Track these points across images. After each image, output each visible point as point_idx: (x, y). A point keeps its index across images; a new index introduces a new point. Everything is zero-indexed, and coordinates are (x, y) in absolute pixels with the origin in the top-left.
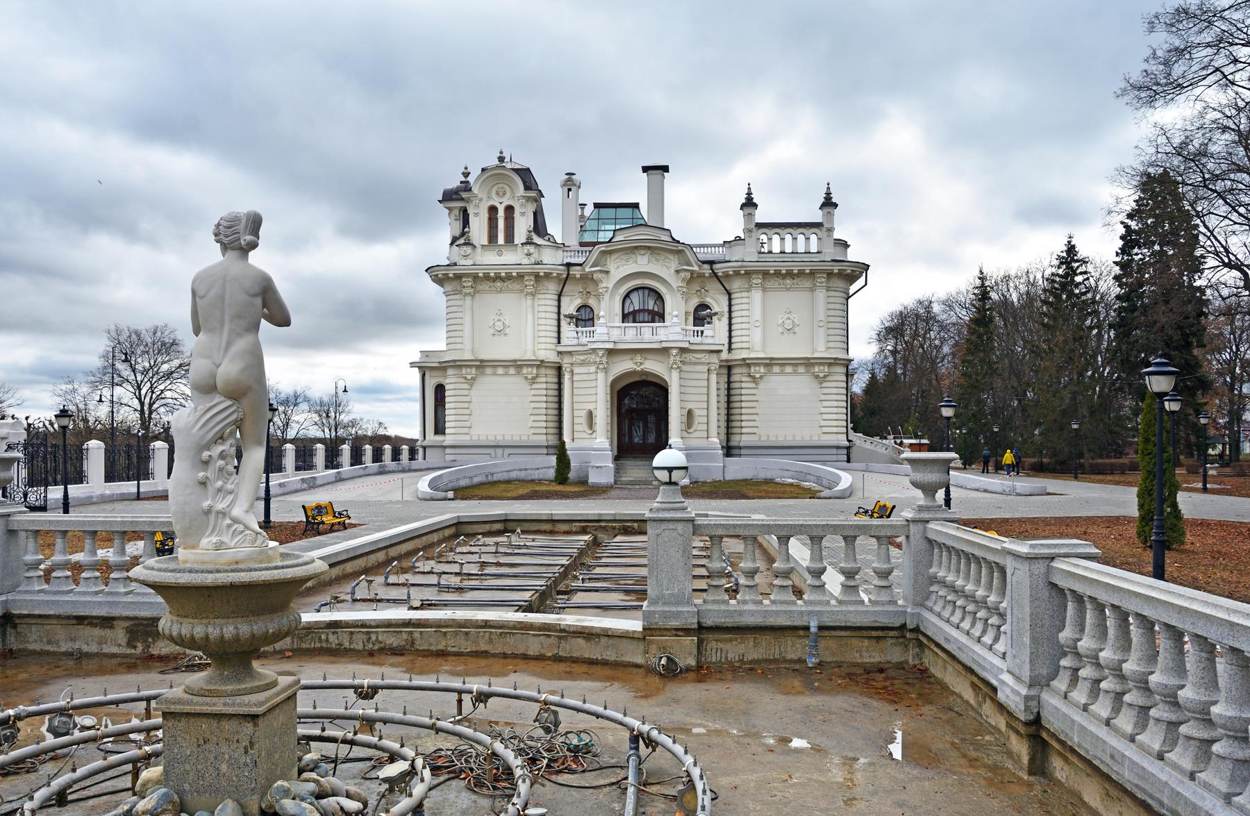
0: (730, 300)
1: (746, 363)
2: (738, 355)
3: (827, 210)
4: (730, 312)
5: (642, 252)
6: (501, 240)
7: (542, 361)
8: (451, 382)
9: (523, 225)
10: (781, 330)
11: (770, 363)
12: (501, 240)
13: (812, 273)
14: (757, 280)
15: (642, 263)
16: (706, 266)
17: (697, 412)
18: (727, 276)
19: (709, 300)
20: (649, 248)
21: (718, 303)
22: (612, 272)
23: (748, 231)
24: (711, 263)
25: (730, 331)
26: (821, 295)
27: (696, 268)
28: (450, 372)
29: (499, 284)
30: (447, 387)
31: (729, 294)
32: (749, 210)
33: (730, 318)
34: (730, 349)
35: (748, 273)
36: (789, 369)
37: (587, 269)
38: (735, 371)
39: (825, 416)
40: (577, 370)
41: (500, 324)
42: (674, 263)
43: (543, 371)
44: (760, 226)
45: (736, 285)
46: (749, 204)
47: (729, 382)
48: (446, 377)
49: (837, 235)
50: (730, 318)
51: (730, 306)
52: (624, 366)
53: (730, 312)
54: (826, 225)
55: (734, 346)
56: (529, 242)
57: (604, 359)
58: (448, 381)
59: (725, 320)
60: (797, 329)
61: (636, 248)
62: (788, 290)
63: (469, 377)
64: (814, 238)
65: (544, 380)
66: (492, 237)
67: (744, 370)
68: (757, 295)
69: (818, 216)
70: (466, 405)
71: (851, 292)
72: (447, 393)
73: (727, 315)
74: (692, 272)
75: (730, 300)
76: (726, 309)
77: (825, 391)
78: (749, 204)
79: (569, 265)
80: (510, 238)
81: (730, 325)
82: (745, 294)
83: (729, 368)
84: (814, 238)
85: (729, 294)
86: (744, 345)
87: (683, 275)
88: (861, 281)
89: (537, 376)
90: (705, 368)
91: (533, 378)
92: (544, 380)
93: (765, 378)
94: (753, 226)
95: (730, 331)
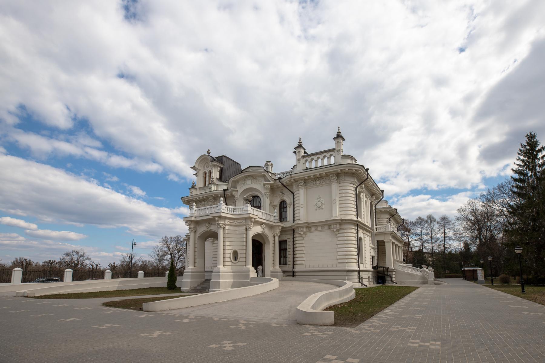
0: (294, 196)
4: (294, 202)
5: (249, 178)
10: (315, 208)
11: (309, 226)
13: (328, 175)
19: (285, 198)
21: (288, 200)
24: (280, 178)
26: (335, 186)
27: (272, 182)
29: (203, 203)
34: (294, 220)
35: (296, 181)
39: (339, 253)
47: (294, 238)
53: (294, 202)
60: (323, 207)
69: (332, 145)
74: (271, 184)
77: (339, 239)
79: (224, 190)
81: (294, 208)
83: (294, 231)
85: (293, 194)
87: (267, 186)
90: (244, 228)
93: (308, 234)
94: (300, 157)
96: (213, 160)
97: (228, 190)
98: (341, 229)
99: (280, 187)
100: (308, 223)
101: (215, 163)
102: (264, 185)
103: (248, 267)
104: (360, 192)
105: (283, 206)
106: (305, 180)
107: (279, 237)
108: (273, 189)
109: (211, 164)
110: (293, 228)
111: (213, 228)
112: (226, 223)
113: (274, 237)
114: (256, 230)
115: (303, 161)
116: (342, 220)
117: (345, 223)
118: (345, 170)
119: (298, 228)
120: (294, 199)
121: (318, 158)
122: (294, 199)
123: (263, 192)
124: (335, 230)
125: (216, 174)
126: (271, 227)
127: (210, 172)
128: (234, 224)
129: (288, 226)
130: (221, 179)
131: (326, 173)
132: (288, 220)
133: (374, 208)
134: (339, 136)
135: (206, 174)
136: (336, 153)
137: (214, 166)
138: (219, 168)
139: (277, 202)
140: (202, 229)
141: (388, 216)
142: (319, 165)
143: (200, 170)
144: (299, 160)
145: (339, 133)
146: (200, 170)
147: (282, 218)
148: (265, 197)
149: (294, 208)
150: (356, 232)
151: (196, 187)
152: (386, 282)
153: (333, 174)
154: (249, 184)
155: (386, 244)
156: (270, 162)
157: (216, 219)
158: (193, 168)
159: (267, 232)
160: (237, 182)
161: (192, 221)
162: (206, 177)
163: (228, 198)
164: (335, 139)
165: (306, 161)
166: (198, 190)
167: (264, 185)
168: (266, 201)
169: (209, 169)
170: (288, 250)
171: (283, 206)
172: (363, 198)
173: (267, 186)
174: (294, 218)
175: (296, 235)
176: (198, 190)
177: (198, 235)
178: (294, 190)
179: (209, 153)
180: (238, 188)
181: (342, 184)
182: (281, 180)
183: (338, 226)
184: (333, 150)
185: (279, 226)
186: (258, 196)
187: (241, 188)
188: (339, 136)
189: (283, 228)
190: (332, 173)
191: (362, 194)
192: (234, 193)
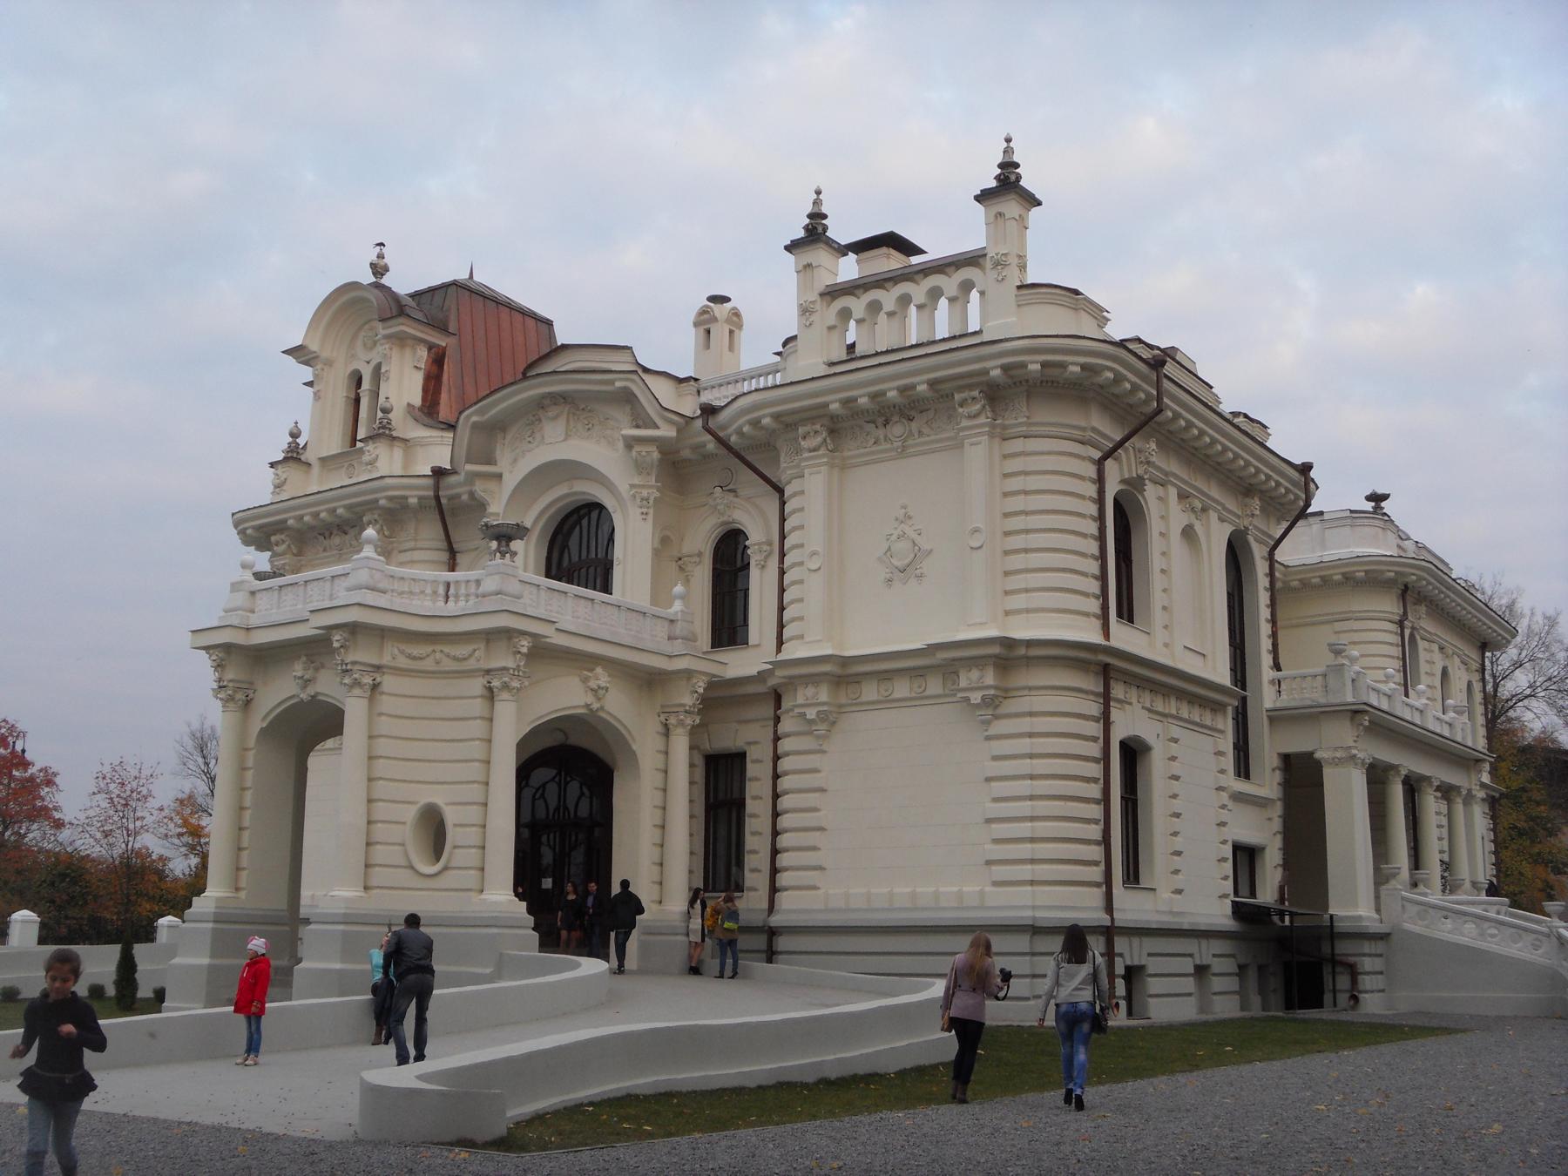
11: (845, 674)
26: (978, 454)
27: (666, 431)
34: (780, 642)
36: (901, 689)
61: (543, 404)
62: (903, 452)
79: (438, 473)
83: (778, 698)
85: (781, 491)
94: (814, 296)
96: (396, 308)
97: (453, 472)
98: (1006, 693)
99: (707, 457)
100: (846, 661)
101: (403, 327)
102: (630, 443)
104: (1134, 485)
105: (730, 557)
106: (833, 418)
107: (694, 731)
108: (678, 469)
109: (382, 330)
110: (772, 682)
111: (328, 686)
112: (386, 660)
113: (667, 732)
114: (563, 696)
115: (830, 313)
116: (1008, 643)
117: (1030, 661)
118: (1023, 365)
119: (792, 682)
121: (935, 294)
122: (783, 520)
123: (623, 487)
124: (976, 697)
125: (404, 385)
126: (649, 681)
127: (377, 373)
128: (428, 664)
129: (753, 671)
130: (429, 410)
131: (933, 384)
132: (753, 637)
133: (1261, 568)
134: (1008, 186)
135: (358, 380)
137: (401, 340)
138: (423, 353)
139: (701, 539)
140: (278, 691)
141: (1390, 606)
142: (942, 331)
143: (329, 363)
144: (805, 311)
145: (1008, 167)
146: (329, 363)
147: (728, 626)
148: (634, 512)
150: (1094, 709)
151: (310, 456)
152: (1328, 998)
153: (970, 387)
154: (558, 443)
155: (1328, 773)
156: (724, 299)
158: (296, 352)
159: (619, 705)
160: (495, 429)
161: (228, 648)
162: (357, 401)
163: (446, 517)
164: (983, 197)
165: (845, 314)
166: (316, 469)
168: (633, 542)
170: (750, 806)
171: (730, 557)
172: (1163, 516)
173: (643, 449)
174: (781, 626)
175: (786, 725)
176: (316, 469)
178: (784, 473)
179: (379, 269)
180: (503, 465)
181: (1018, 445)
182: (713, 423)
183: (990, 678)
184: (973, 260)
185: (688, 674)
186: (599, 507)
187: (517, 462)
188: (1008, 186)
189: (715, 684)
190: (965, 382)
191: (1151, 492)
192: (479, 487)
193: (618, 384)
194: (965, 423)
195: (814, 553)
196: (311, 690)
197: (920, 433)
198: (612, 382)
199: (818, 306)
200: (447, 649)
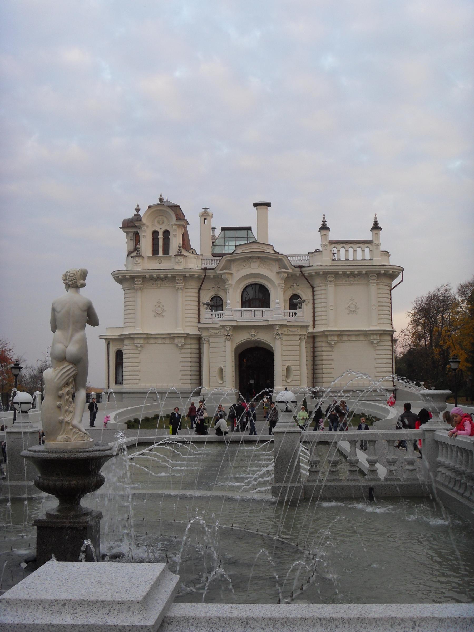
0: (313, 291)
1: (325, 334)
2: (319, 329)
3: (375, 231)
4: (314, 300)
6: (161, 253)
7: (188, 334)
8: (127, 349)
9: (175, 242)
11: (341, 334)
12: (161, 253)
14: (330, 278)
15: (255, 268)
16: (298, 269)
17: (293, 368)
18: (311, 275)
19: (299, 292)
20: (259, 257)
21: (305, 295)
22: (235, 274)
23: (324, 246)
24: (300, 267)
25: (314, 312)
26: (373, 288)
27: (290, 271)
28: (126, 342)
30: (124, 352)
31: (313, 288)
32: (324, 232)
33: (314, 304)
37: (218, 272)
38: (317, 340)
40: (211, 340)
41: (160, 309)
42: (276, 268)
43: (189, 341)
44: (332, 243)
45: (317, 282)
46: (324, 227)
48: (123, 345)
49: (382, 248)
50: (314, 304)
51: (313, 295)
52: (243, 337)
53: (314, 300)
54: (375, 242)
55: (316, 323)
56: (179, 254)
57: (230, 333)
58: (125, 348)
59: (310, 306)
62: (352, 284)
63: (139, 345)
64: (367, 250)
65: (189, 347)
66: (155, 252)
67: (323, 339)
68: (331, 288)
70: (136, 364)
71: (393, 286)
72: (124, 356)
73: (311, 302)
74: (288, 274)
75: (313, 291)
76: (311, 298)
78: (324, 227)
79: (205, 269)
80: (166, 251)
81: (314, 308)
82: (322, 288)
84: (367, 250)
85: (313, 288)
86: (324, 322)
87: (282, 275)
88: (399, 279)
89: (185, 344)
91: (182, 346)
92: (189, 347)
94: (327, 243)
95: (314, 312)
103: (302, 387)
120: (313, 295)
136: (375, 247)
149: (314, 308)
157: (277, 327)
167: (278, 273)
169: (165, 228)
176: (146, 260)
177: (235, 345)
182: (304, 269)
190: (373, 272)
193: (280, 257)
194: (371, 281)
195: (331, 305)
196: (256, 338)
197: (358, 281)
198: (278, 257)
199: (328, 245)
200: (290, 329)
